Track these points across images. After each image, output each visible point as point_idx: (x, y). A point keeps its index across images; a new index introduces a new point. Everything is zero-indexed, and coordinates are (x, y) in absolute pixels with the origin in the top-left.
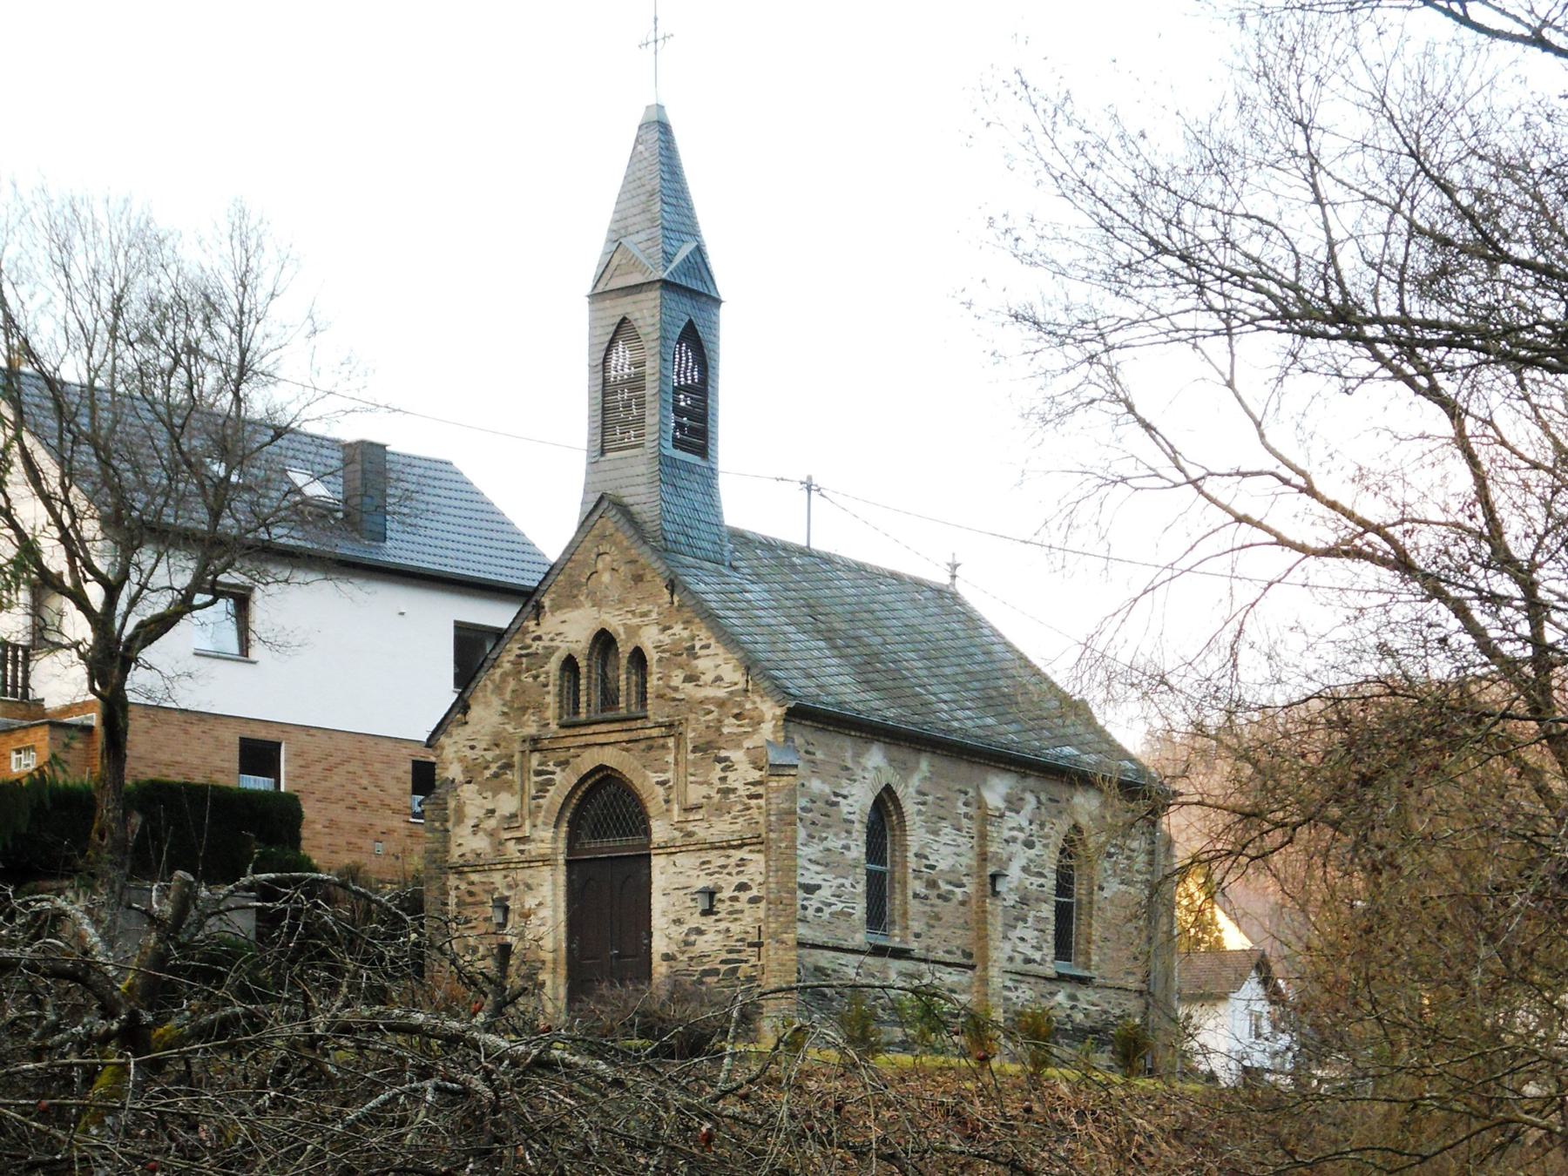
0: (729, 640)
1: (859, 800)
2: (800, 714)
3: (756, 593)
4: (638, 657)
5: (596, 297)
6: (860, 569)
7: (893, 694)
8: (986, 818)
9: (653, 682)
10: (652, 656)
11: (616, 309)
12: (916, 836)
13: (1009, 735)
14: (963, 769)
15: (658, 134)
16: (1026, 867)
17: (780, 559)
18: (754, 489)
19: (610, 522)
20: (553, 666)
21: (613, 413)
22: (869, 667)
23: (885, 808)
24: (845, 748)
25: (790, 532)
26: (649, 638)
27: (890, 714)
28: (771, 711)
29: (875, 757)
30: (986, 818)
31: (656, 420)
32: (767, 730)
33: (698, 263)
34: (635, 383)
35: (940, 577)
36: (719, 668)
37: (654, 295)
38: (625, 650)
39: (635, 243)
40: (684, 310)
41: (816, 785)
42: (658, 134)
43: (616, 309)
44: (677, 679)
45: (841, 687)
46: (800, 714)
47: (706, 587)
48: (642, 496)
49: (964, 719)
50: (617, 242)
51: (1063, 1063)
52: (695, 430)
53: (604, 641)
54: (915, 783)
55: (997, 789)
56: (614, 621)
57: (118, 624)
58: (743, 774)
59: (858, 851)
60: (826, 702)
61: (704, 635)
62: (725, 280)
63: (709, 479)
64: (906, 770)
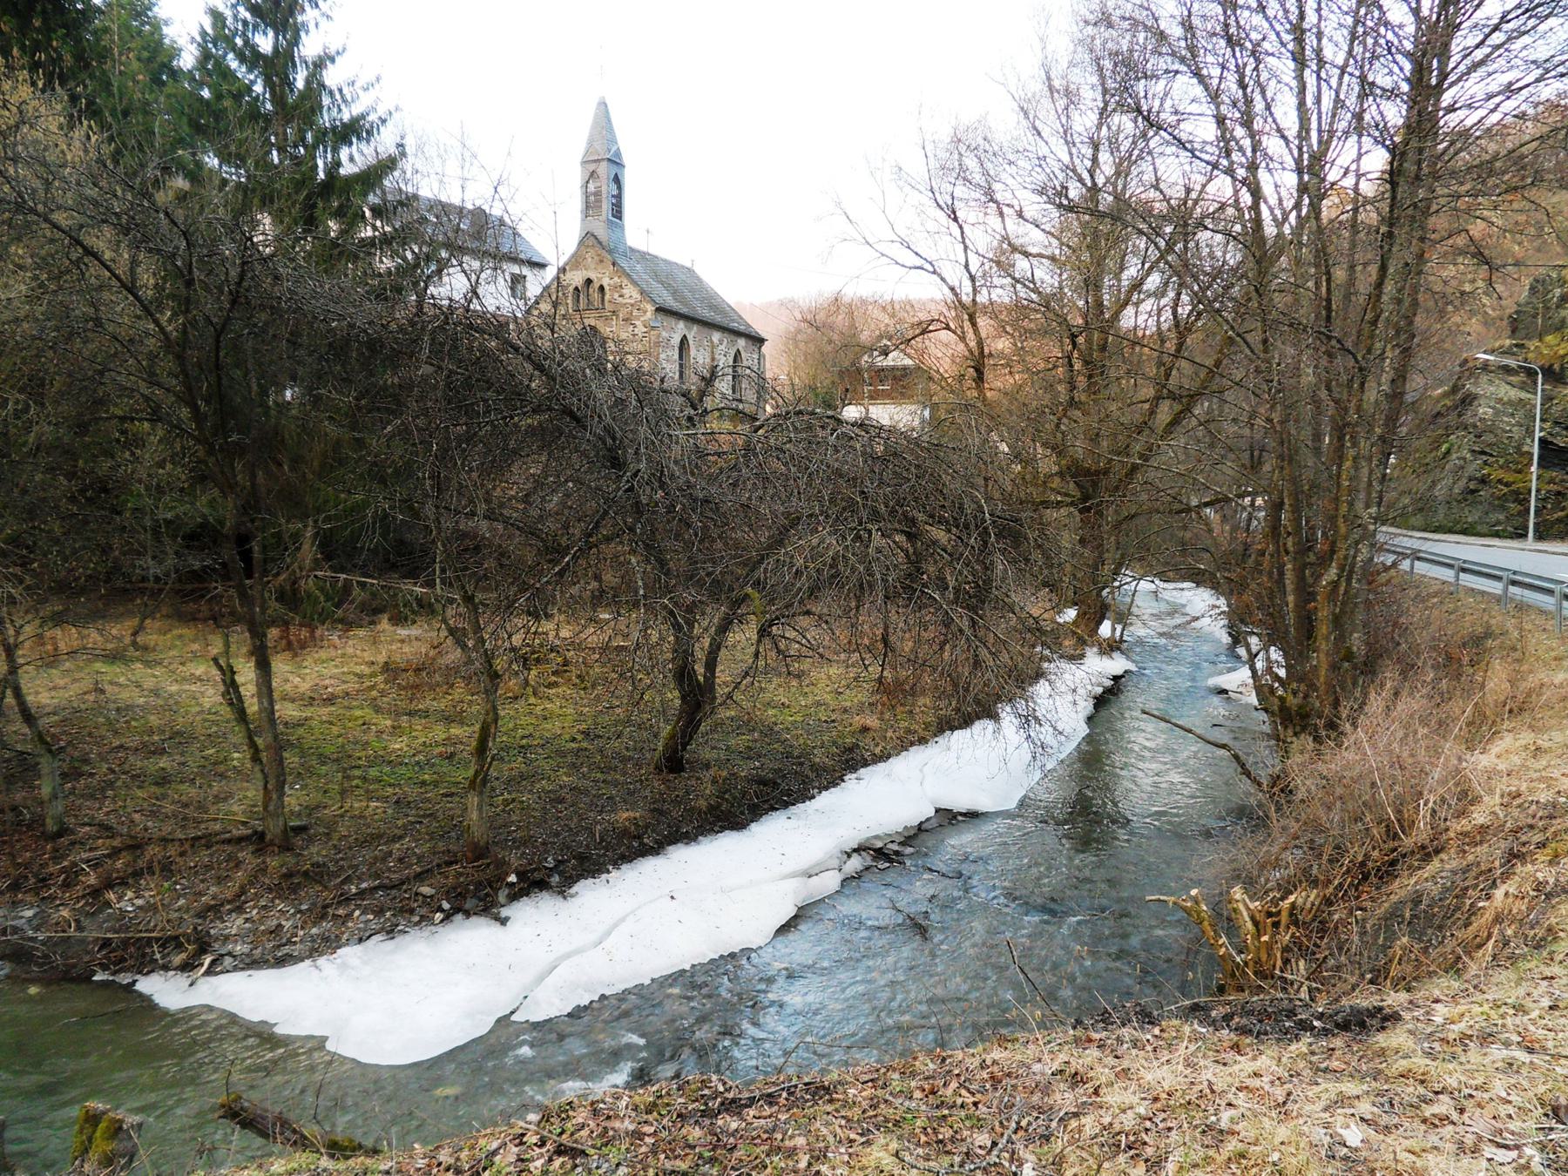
0: (635, 283)
1: (676, 340)
2: (661, 310)
3: (638, 267)
4: (602, 288)
5: (584, 163)
6: (665, 261)
7: (685, 304)
8: (713, 347)
9: (607, 297)
10: (607, 288)
11: (592, 167)
12: (693, 352)
13: (718, 319)
14: (706, 330)
15: (603, 105)
16: (725, 361)
17: (644, 257)
18: (639, 232)
19: (591, 241)
20: (571, 289)
21: (590, 205)
22: (675, 293)
23: (684, 339)
24: (672, 321)
25: (643, 248)
26: (606, 282)
27: (684, 310)
28: (650, 308)
29: (681, 324)
30: (713, 347)
31: (606, 207)
32: (649, 314)
33: (618, 153)
34: (597, 194)
35: (688, 265)
36: (631, 293)
37: (605, 164)
38: (596, 285)
39: (597, 146)
40: (614, 170)
41: (664, 334)
42: (603, 105)
43: (592, 167)
44: (616, 296)
45: (671, 303)
46: (661, 310)
47: (624, 264)
48: (601, 231)
49: (706, 314)
50: (590, 143)
51: (1114, 630)
52: (618, 212)
53: (589, 281)
54: (693, 333)
55: (716, 336)
56: (593, 276)
57: (1451, 65)
58: (640, 329)
59: (676, 356)
60: (667, 306)
61: (625, 281)
62: (626, 159)
63: (622, 228)
64: (690, 329)
